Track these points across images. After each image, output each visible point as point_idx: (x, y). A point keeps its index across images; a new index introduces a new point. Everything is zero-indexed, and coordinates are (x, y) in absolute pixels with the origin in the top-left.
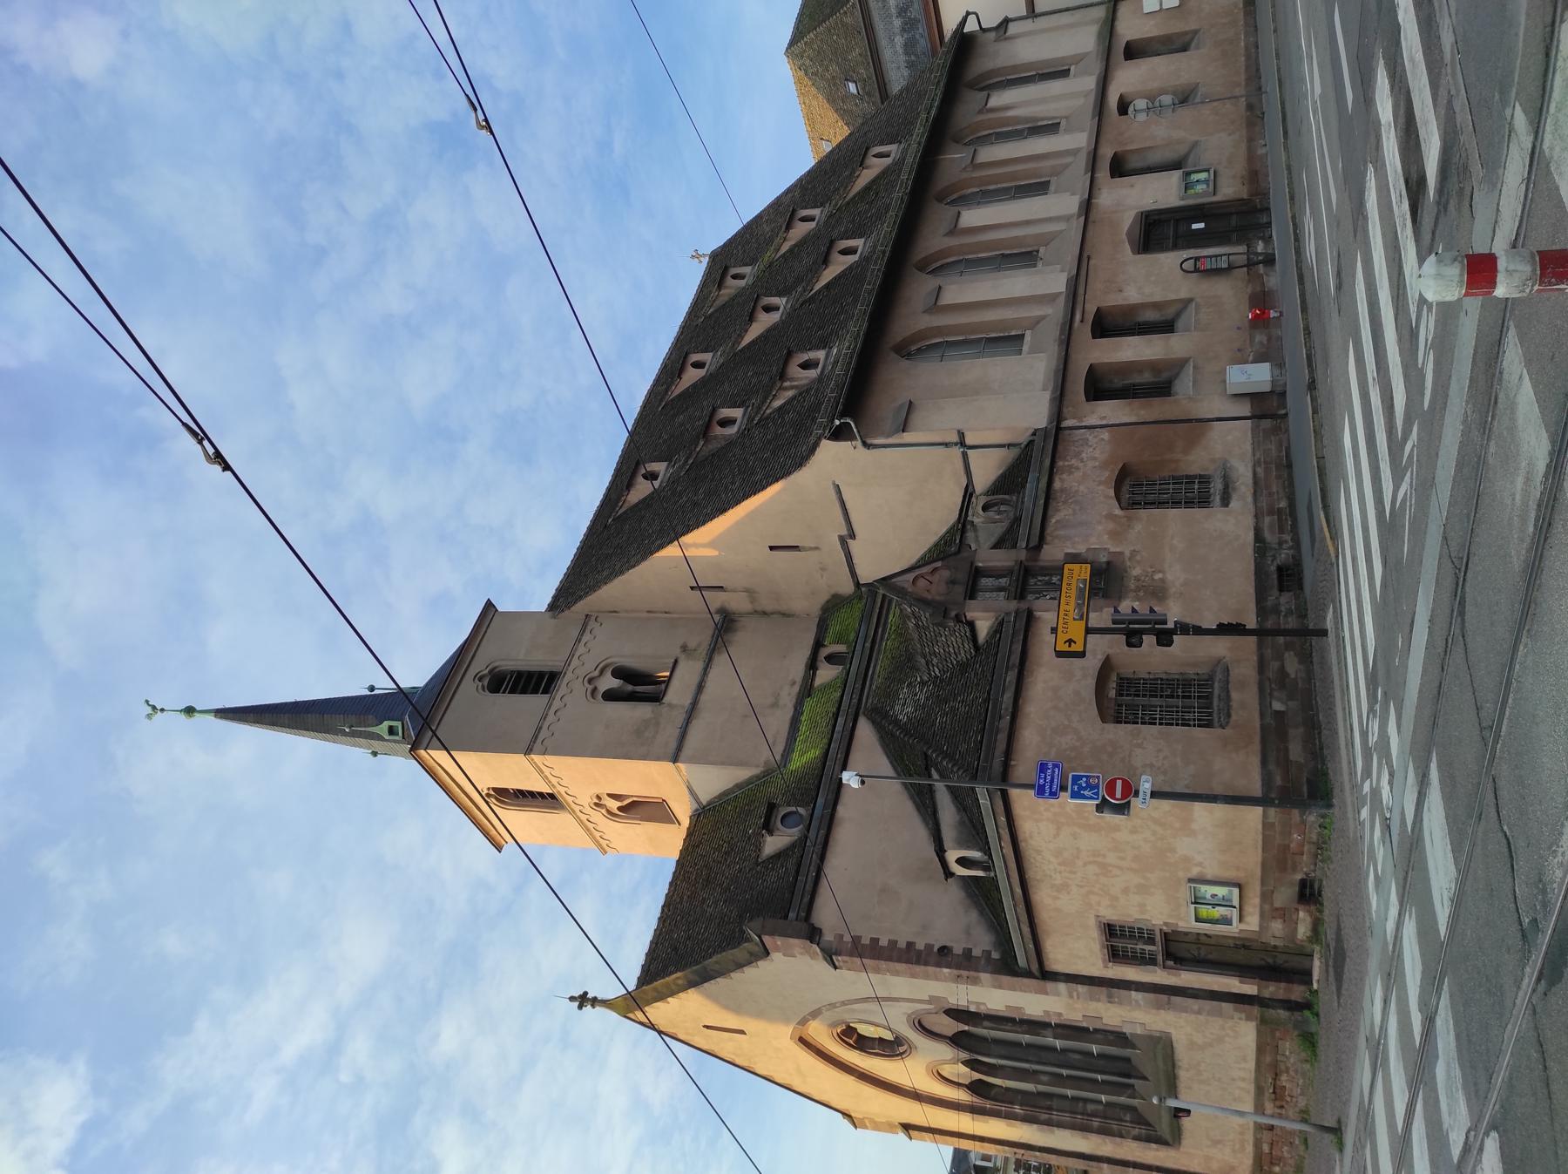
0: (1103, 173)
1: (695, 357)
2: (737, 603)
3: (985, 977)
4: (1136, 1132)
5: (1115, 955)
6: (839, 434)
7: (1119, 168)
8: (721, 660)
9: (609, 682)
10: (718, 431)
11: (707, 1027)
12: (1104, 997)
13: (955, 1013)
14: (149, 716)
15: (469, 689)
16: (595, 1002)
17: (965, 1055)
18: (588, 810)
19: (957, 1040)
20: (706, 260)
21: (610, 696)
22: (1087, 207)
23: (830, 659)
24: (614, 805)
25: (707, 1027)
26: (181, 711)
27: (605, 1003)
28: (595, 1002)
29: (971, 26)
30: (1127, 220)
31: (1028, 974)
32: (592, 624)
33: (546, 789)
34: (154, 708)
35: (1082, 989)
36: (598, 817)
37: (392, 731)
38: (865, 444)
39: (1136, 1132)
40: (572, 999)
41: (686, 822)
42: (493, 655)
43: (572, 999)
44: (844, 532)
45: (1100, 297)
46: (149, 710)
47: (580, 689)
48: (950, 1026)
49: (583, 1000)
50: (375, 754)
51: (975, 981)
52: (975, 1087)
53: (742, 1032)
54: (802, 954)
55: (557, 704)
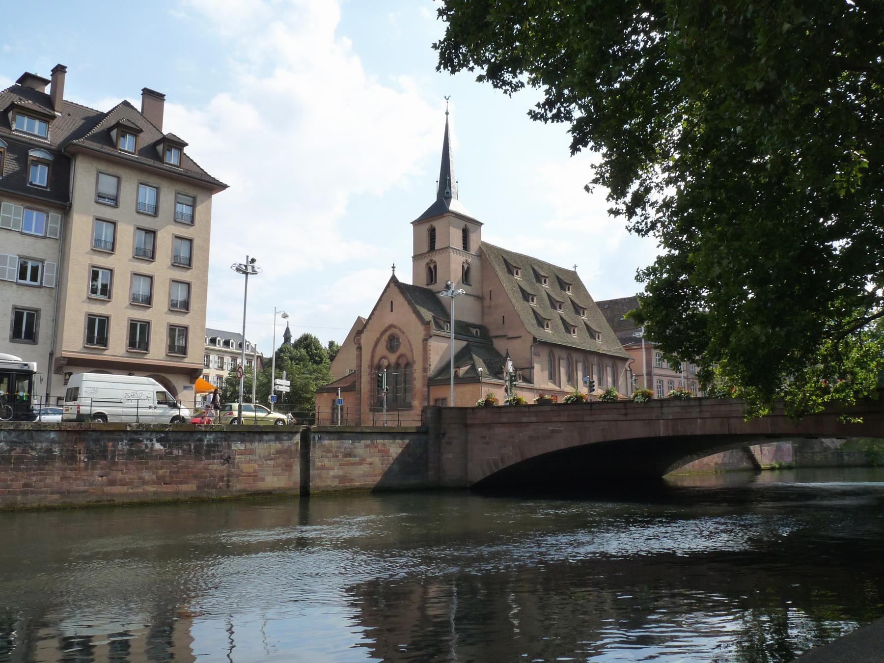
1: (547, 280)
2: (487, 302)
4: (372, 402)
8: (472, 298)
10: (531, 297)
11: (392, 302)
12: (424, 397)
13: (408, 365)
14: (445, 97)
16: (393, 271)
17: (393, 365)
19: (398, 365)
20: (573, 269)
21: (463, 266)
23: (477, 332)
24: (432, 266)
25: (392, 302)
27: (394, 273)
28: (393, 271)
31: (428, 383)
32: (479, 258)
33: (436, 248)
34: (447, 99)
35: (426, 393)
36: (427, 260)
37: (448, 193)
38: (532, 346)
39: (372, 402)
42: (470, 226)
44: (508, 336)
46: (447, 98)
47: (464, 259)
48: (403, 362)
49: (394, 267)
50: (437, 182)
52: (379, 367)
53: (392, 311)
55: (461, 253)
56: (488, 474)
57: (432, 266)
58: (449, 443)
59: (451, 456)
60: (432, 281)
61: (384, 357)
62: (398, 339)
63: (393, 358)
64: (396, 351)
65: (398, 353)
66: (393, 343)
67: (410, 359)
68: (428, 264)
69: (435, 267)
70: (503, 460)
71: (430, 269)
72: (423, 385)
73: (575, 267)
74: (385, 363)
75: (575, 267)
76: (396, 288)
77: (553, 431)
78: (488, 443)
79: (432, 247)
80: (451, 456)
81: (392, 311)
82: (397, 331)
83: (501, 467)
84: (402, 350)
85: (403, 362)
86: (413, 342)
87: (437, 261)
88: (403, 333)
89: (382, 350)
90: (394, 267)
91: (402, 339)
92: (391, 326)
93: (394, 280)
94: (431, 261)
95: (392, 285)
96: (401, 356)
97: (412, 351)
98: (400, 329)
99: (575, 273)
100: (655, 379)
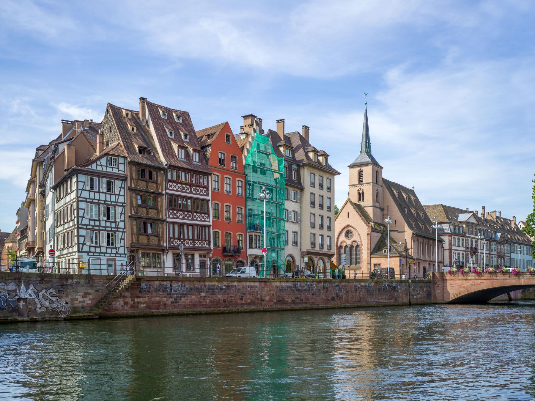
0: (429, 262)
2: (385, 212)
3: (369, 251)
5: (375, 265)
6: (413, 234)
7: (429, 264)
9: (377, 192)
11: (348, 213)
13: (358, 246)
15: (376, 168)
18: (359, 187)
19: (352, 246)
20: (412, 189)
22: (427, 261)
29: (443, 242)
30: (425, 265)
33: (364, 182)
35: (370, 261)
36: (358, 188)
41: (359, 203)
42: (379, 169)
45: (421, 263)
48: (355, 246)
51: (368, 250)
53: (348, 217)
56: (454, 298)
57: (361, 192)
58: (438, 286)
59: (439, 291)
60: (360, 200)
61: (344, 242)
62: (351, 232)
63: (349, 242)
64: (351, 239)
65: (352, 240)
66: (348, 234)
67: (359, 243)
68: (358, 190)
69: (363, 193)
70: (459, 293)
71: (359, 193)
73: (413, 187)
74: (344, 245)
75: (413, 187)
76: (351, 205)
77: (481, 283)
78: (453, 287)
79: (360, 181)
80: (439, 291)
81: (348, 217)
82: (352, 229)
83: (459, 296)
84: (355, 237)
85: (355, 246)
87: (364, 189)
88: (355, 229)
89: (343, 238)
90: (349, 194)
92: (348, 226)
93: (349, 200)
94: (361, 189)
95: (348, 203)
96: (354, 241)
98: (353, 228)
99: (413, 191)
100: (453, 251)
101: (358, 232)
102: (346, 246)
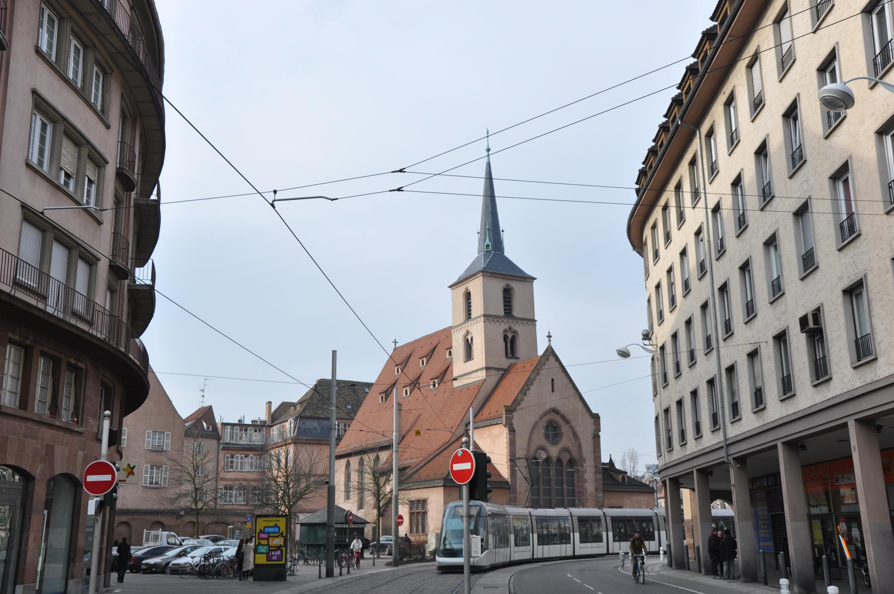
16: (550, 341)
24: (510, 336)
26: (488, 146)
31: (603, 488)
40: (549, 333)
43: (549, 333)
49: (549, 337)
53: (553, 391)
54: (595, 428)
57: (510, 336)
61: (543, 448)
63: (554, 451)
67: (575, 455)
68: (505, 331)
71: (505, 337)
72: (596, 489)
74: (543, 455)
82: (558, 418)
84: (566, 441)
85: (565, 458)
86: (581, 436)
88: (567, 422)
89: (540, 439)
90: (549, 337)
91: (564, 428)
94: (510, 328)
97: (580, 447)
98: (563, 417)
101: (572, 428)
102: (548, 460)
